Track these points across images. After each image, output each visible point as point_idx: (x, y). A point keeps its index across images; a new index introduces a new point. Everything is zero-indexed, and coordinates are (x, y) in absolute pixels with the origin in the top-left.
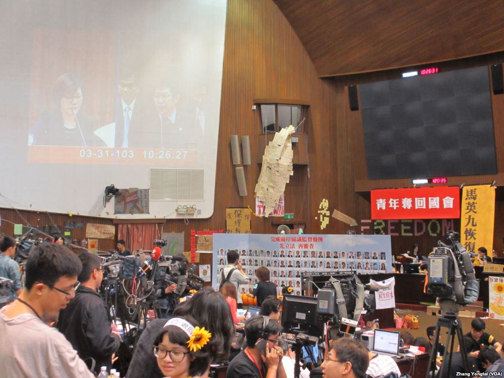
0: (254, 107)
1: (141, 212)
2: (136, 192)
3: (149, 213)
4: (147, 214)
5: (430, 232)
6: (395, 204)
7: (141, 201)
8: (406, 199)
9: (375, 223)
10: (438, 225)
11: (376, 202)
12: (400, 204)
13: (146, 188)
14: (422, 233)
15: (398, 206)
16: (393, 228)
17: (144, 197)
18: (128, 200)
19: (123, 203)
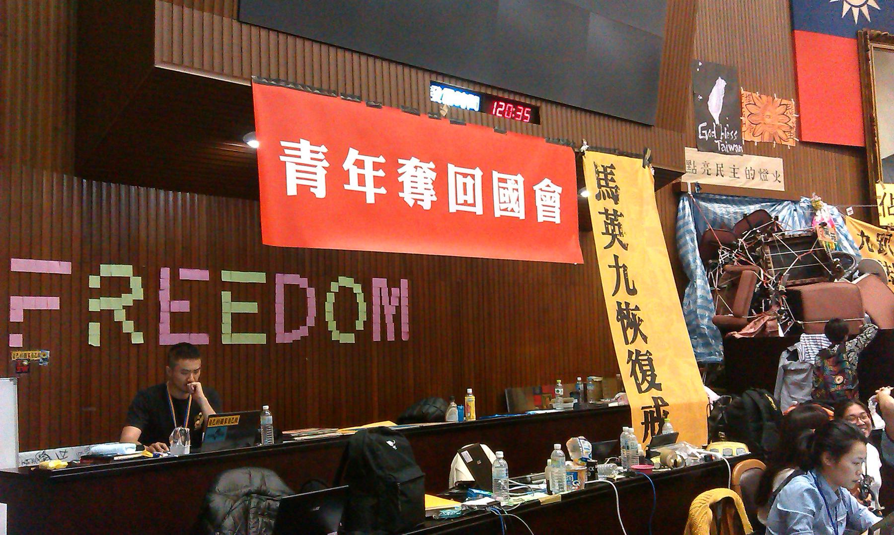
5: (332, 325)
6: (369, 181)
8: (415, 161)
9: (94, 282)
10: (360, 299)
11: (281, 151)
12: (390, 180)
14: (303, 331)
15: (383, 191)
16: (183, 306)
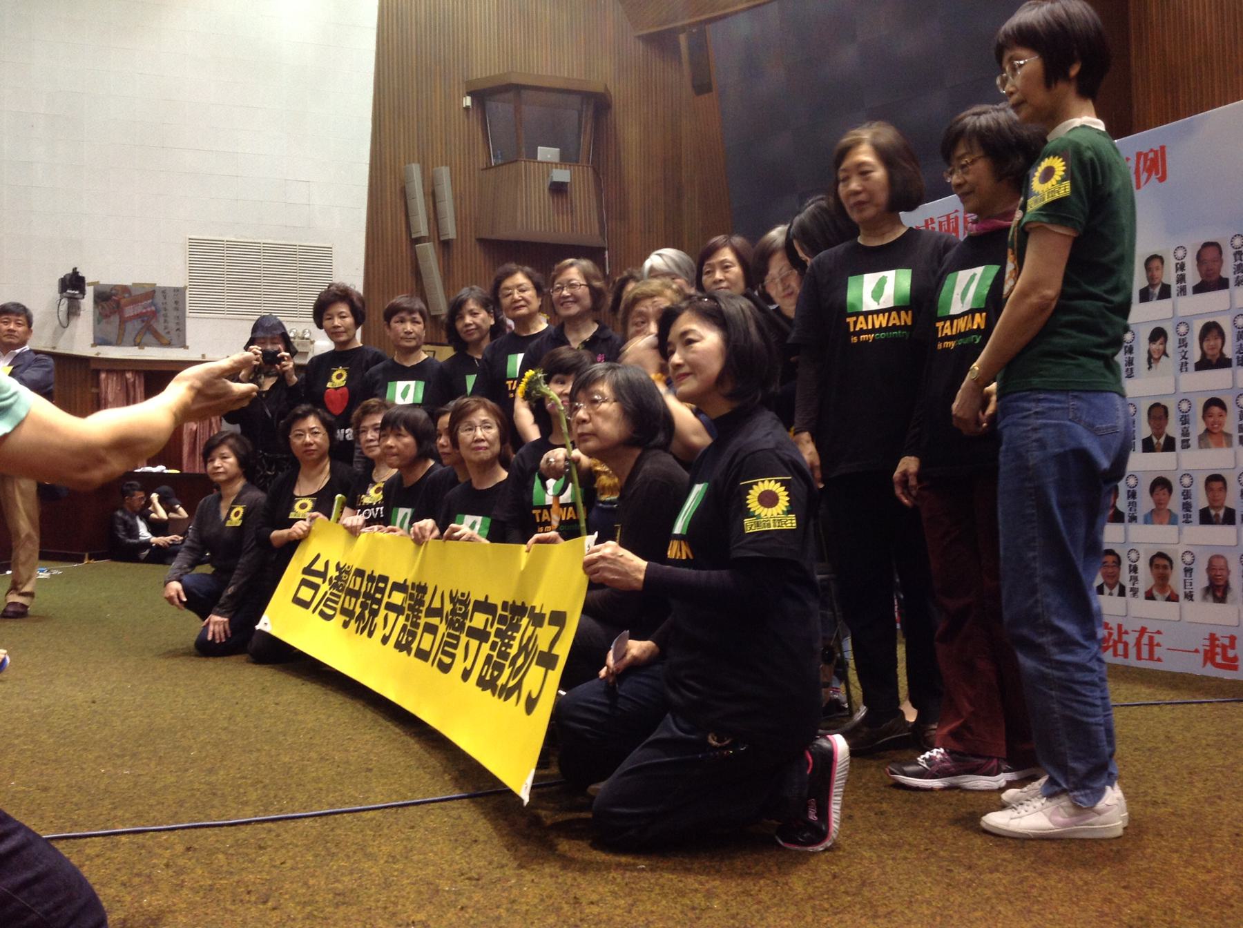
0: (467, 101)
1: (169, 344)
2: (150, 293)
3: (185, 346)
4: (182, 350)
7: (165, 316)
13: (180, 285)
17: (171, 305)
18: (129, 311)
19: (115, 319)
